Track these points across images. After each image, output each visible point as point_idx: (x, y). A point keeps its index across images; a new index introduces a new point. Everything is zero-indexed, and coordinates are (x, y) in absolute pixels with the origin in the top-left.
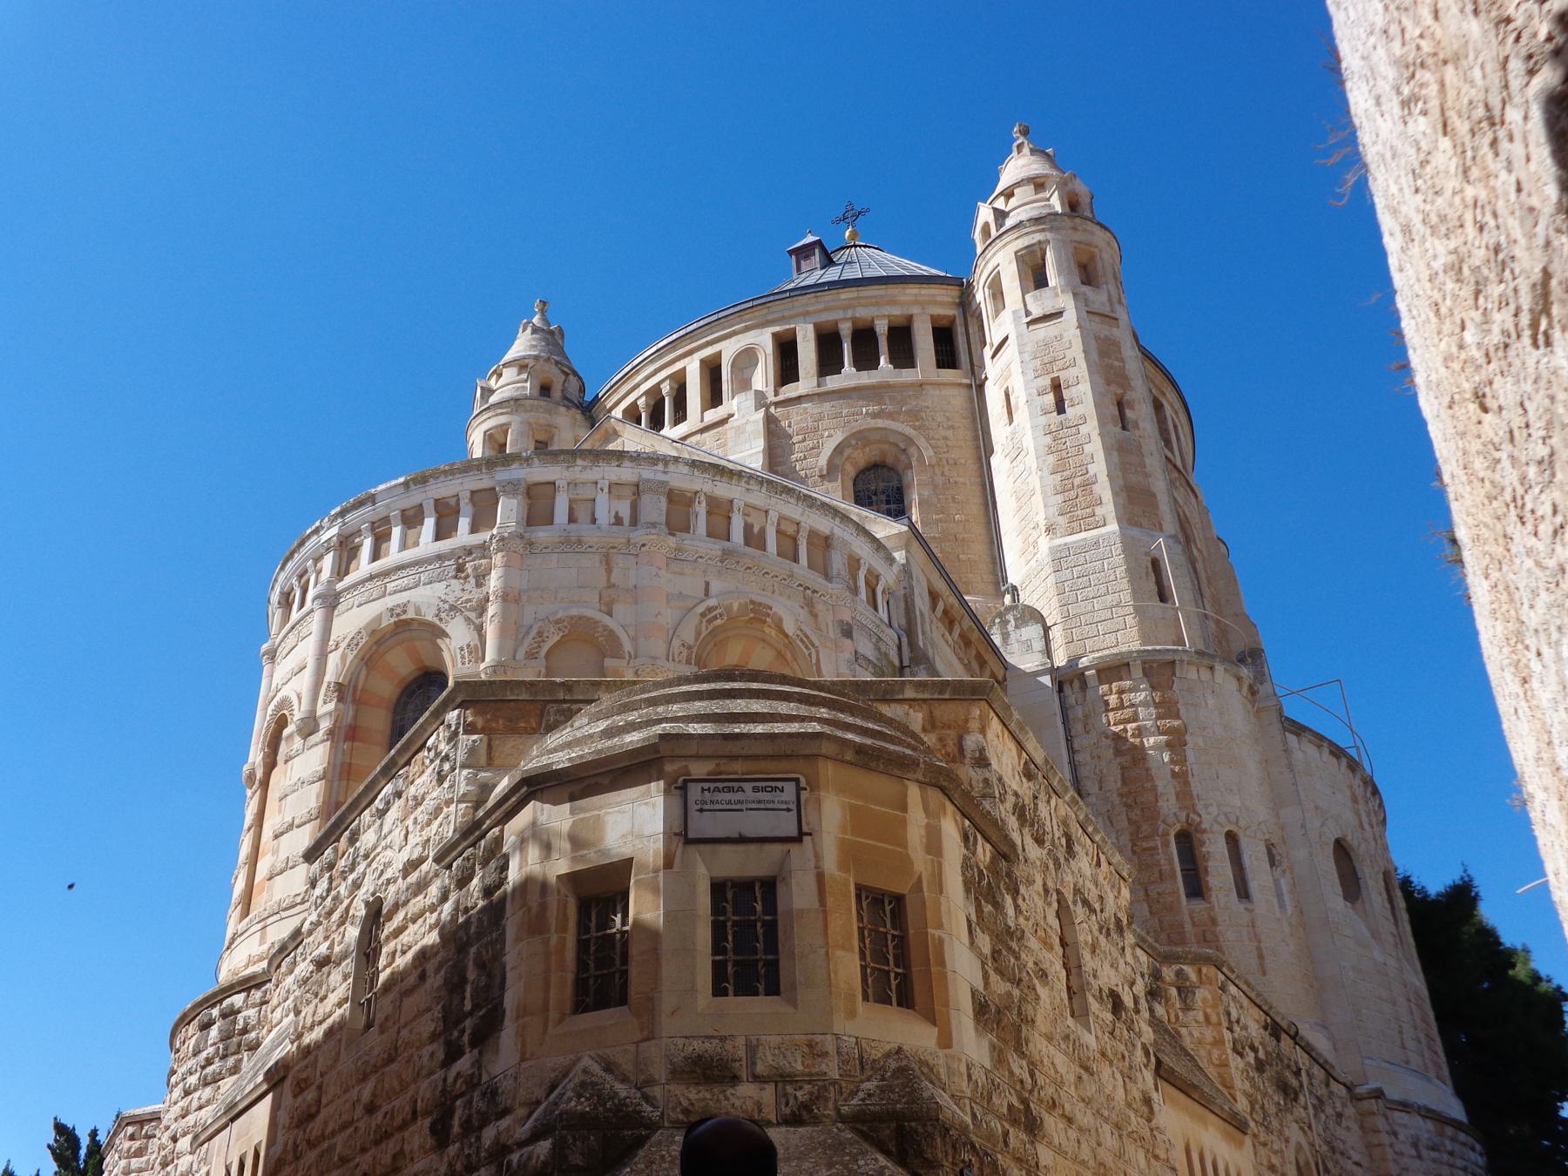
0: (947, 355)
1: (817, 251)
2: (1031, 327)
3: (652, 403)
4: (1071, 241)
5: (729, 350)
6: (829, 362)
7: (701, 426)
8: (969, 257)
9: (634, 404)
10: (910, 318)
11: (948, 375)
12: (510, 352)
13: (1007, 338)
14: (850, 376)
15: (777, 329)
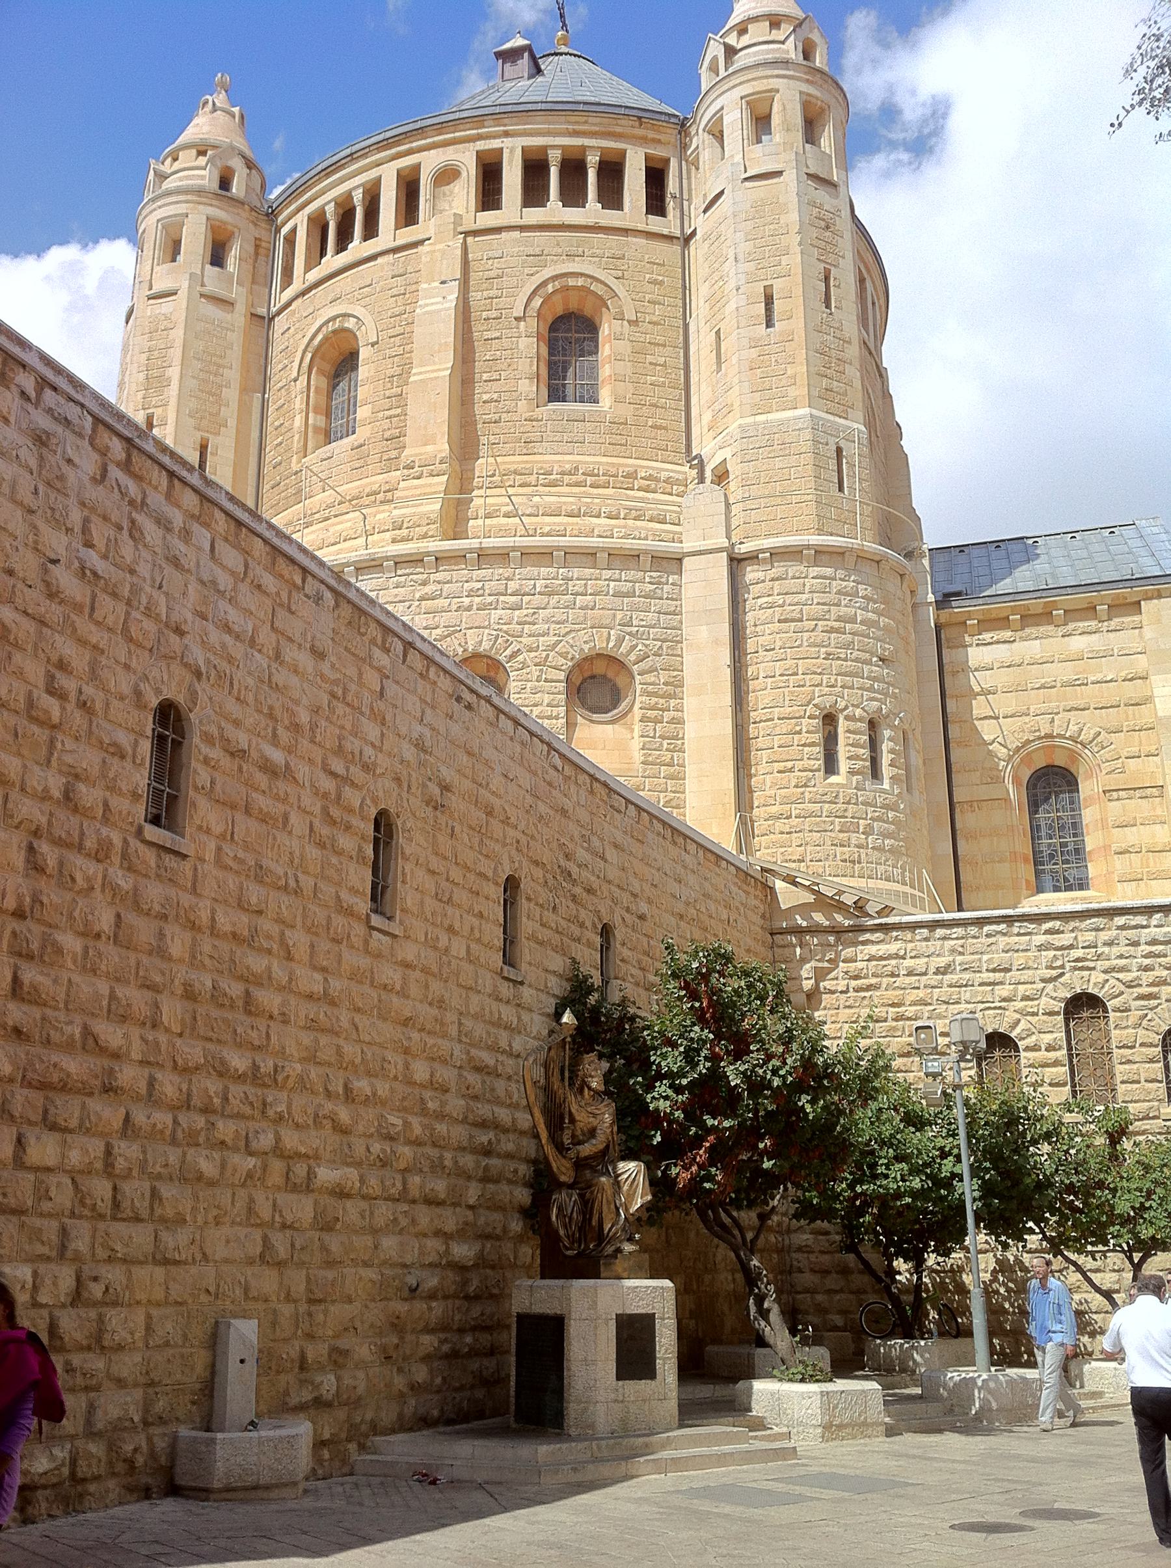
0: (656, 203)
1: (526, 55)
2: (748, 184)
3: (341, 212)
4: (801, 92)
5: (430, 162)
6: (534, 193)
7: (392, 245)
8: (692, 92)
9: (322, 212)
10: (623, 153)
11: (655, 224)
12: (186, 132)
13: (722, 192)
14: (554, 210)
15: (481, 145)
